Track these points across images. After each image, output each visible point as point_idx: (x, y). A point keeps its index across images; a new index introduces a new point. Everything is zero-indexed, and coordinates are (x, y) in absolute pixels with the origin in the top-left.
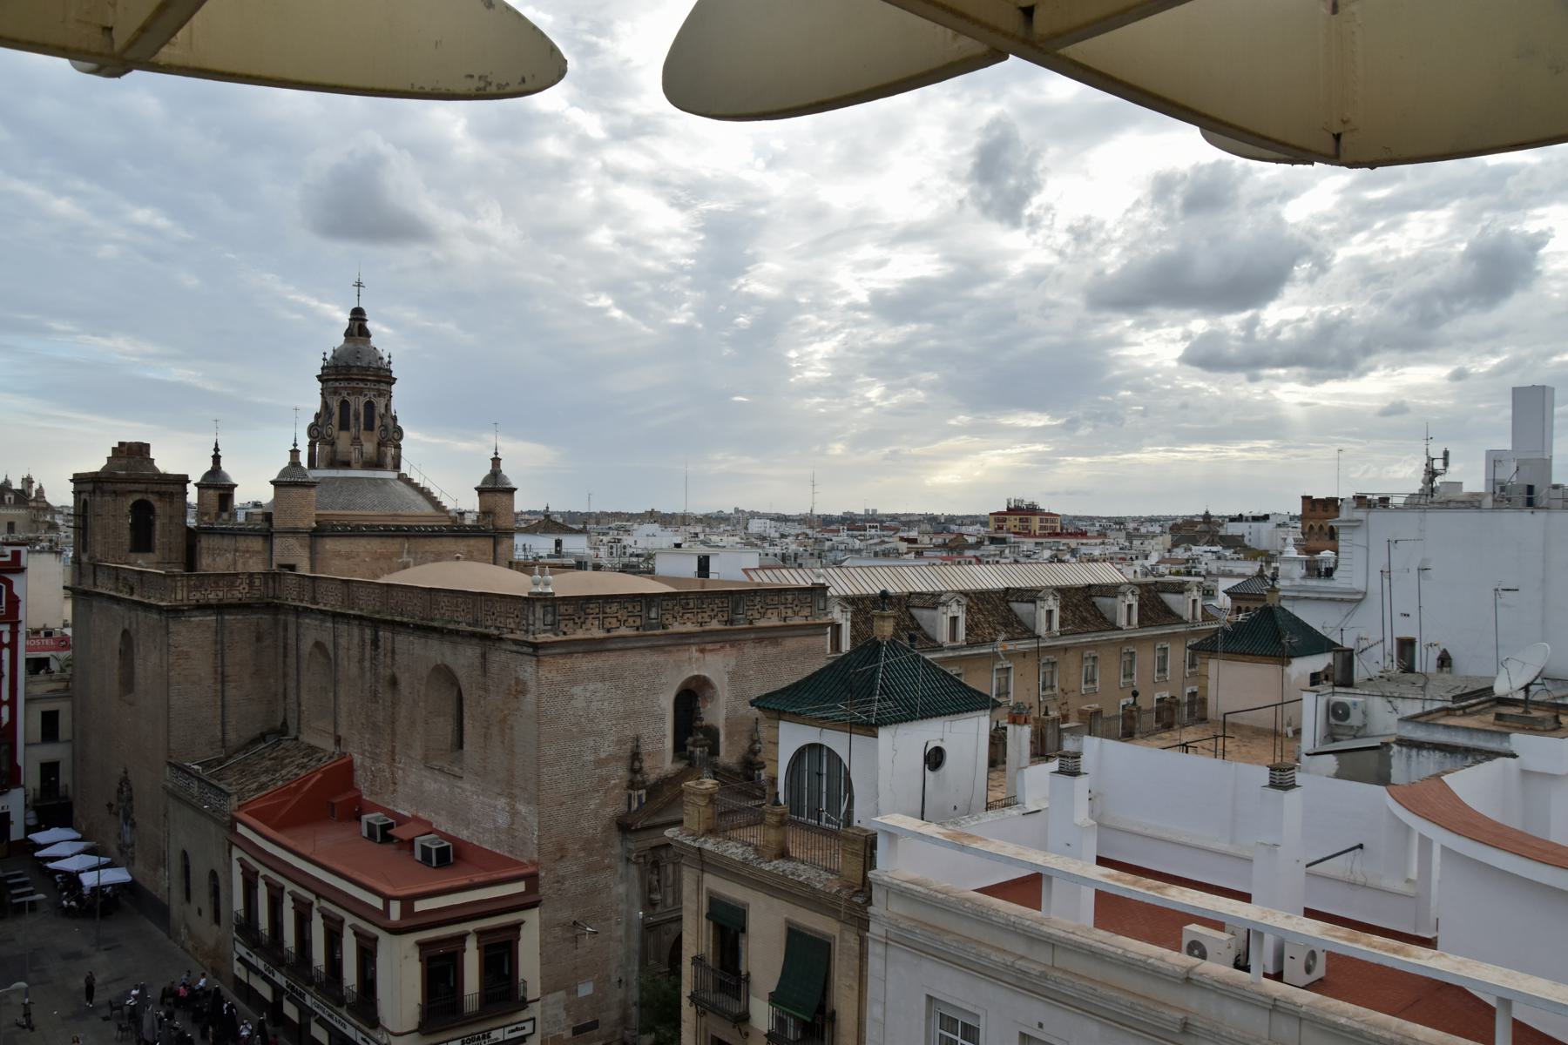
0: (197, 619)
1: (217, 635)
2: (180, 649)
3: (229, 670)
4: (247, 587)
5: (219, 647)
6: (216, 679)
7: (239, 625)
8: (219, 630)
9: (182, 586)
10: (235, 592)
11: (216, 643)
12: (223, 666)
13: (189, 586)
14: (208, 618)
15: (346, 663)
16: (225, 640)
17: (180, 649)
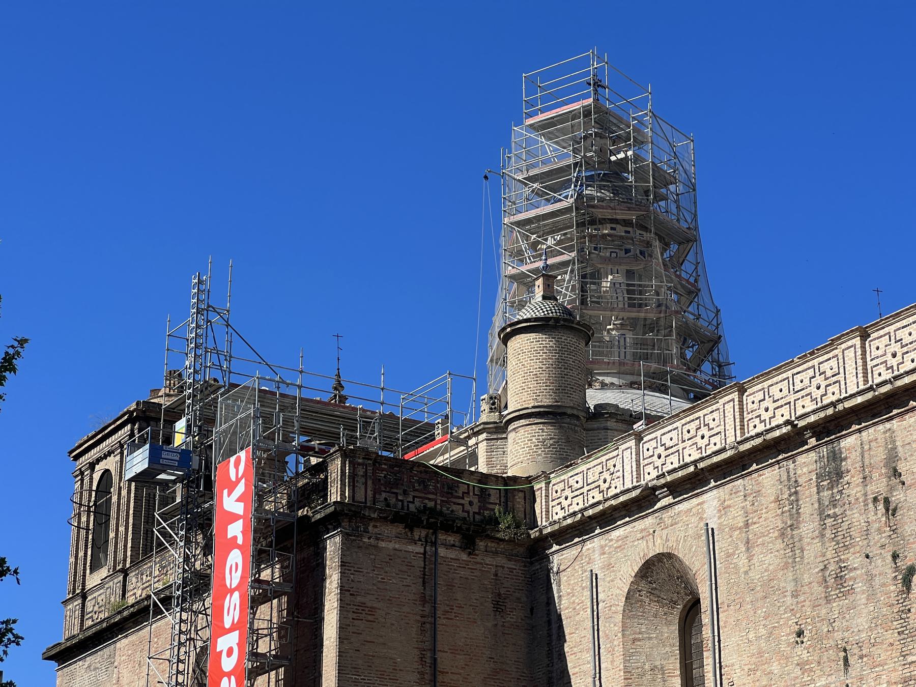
0: (391, 545)
1: (424, 583)
2: (359, 599)
3: (444, 661)
4: (476, 500)
5: (428, 609)
6: (422, 673)
7: (462, 573)
8: (428, 577)
9: (365, 475)
10: (454, 507)
11: (424, 600)
12: (434, 651)
13: (376, 481)
14: (410, 548)
15: (742, 561)
16: (439, 598)
17: (359, 599)
